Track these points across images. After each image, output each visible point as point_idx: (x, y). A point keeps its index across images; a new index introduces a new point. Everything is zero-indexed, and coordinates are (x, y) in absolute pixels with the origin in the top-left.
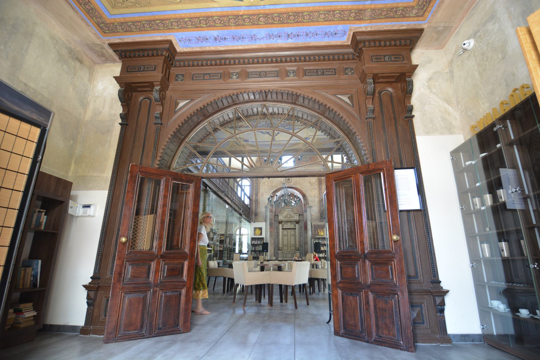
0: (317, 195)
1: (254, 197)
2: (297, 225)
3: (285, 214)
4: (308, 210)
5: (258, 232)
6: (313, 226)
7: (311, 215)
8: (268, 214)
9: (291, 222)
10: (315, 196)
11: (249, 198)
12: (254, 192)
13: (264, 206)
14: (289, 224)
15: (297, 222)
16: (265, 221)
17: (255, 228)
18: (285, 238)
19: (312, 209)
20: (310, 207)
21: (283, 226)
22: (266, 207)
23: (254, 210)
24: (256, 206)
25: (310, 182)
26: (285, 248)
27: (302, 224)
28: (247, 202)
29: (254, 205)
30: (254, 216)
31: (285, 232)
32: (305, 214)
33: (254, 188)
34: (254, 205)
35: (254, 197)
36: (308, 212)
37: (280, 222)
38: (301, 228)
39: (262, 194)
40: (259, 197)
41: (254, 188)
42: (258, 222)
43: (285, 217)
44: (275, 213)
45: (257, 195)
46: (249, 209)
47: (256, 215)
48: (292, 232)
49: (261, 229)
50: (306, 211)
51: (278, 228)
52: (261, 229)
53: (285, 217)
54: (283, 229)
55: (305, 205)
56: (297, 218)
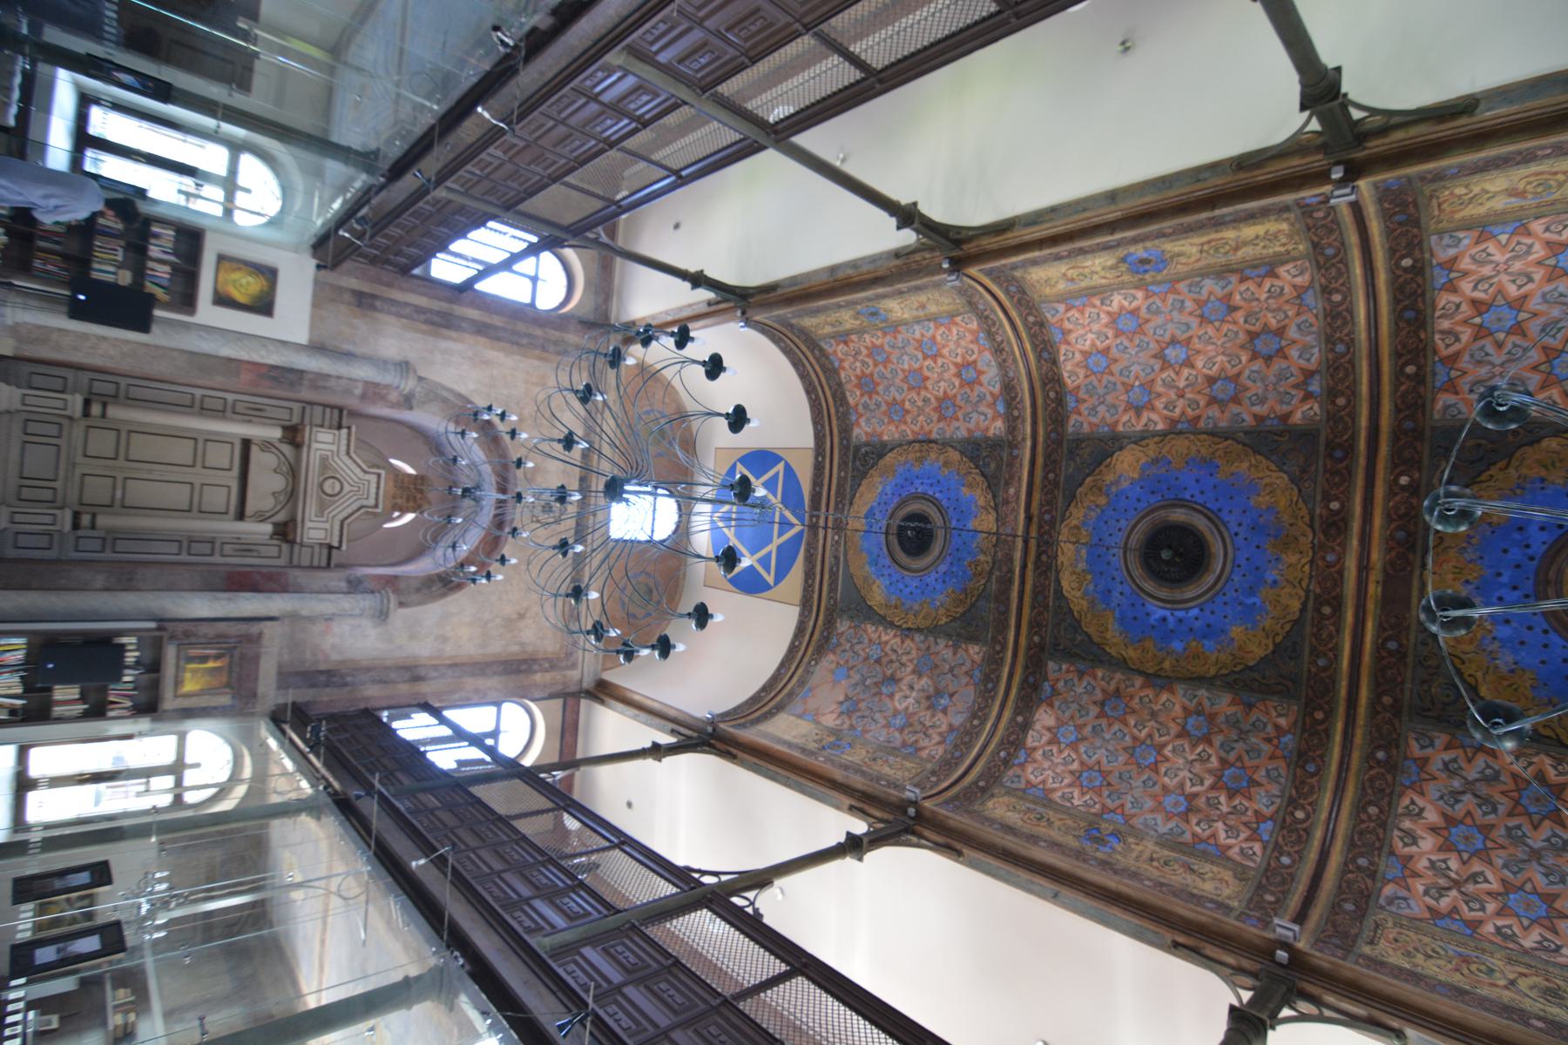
0: (449, 650)
1: (473, 314)
2: (267, 528)
3: (350, 470)
4: (365, 602)
5: (245, 286)
6: (254, 629)
7: (329, 619)
8: (362, 372)
9: (292, 494)
10: (445, 639)
11: (468, 286)
12: (497, 321)
13: (412, 356)
14: (279, 483)
15: (285, 532)
16: (316, 347)
17: (269, 274)
18: (183, 451)
19: (366, 623)
20: (382, 616)
21: (267, 445)
22: (405, 367)
23: (397, 295)
24: (419, 310)
25: (521, 616)
26: (102, 442)
27: (272, 556)
28: (445, 269)
29: (422, 301)
30: (354, 283)
31: (222, 456)
32: (335, 579)
33: (521, 327)
34: (422, 301)
35: (473, 314)
36: (347, 603)
37: (293, 435)
38: (246, 548)
39: (486, 362)
40: (470, 338)
41: (521, 327)
42: (316, 304)
43: (325, 464)
44: (354, 414)
45: (481, 329)
46: (405, 271)
47: (364, 301)
48: (221, 496)
49: (264, 306)
50: (355, 586)
51: (253, 414)
52: (264, 306)
53: (324, 460)
54: (246, 443)
55: (392, 581)
56: (315, 530)
